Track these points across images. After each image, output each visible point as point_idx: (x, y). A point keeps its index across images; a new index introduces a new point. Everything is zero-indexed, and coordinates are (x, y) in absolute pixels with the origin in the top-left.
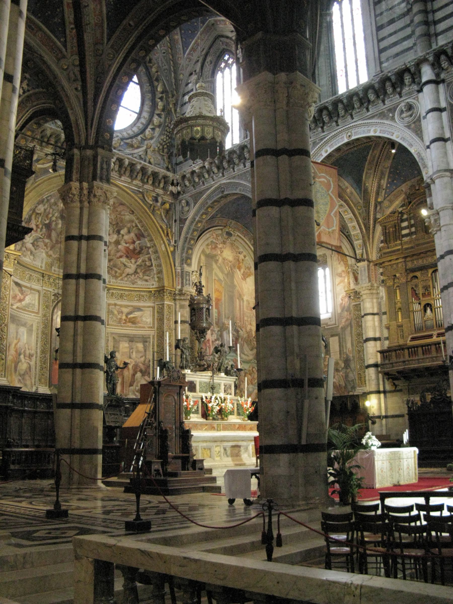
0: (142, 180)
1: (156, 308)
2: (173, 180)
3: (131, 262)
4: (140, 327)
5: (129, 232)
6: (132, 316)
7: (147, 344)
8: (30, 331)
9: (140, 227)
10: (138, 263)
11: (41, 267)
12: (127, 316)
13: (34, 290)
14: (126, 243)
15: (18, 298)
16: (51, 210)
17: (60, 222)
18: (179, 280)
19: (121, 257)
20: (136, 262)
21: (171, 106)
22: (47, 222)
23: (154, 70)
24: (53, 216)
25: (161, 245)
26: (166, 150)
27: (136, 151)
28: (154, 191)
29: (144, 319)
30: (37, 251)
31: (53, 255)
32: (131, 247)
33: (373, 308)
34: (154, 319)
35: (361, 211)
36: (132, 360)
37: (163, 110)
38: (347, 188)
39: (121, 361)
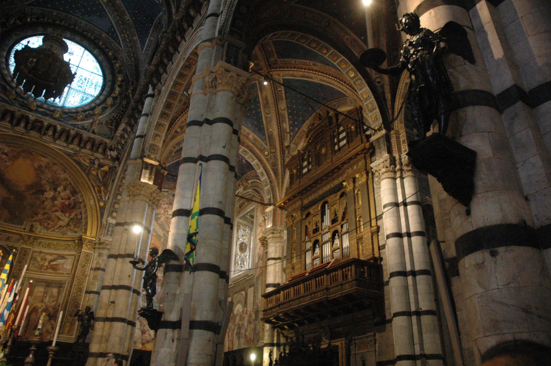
0: (79, 145)
2: (112, 146)
3: (65, 216)
4: (60, 273)
5: (65, 189)
6: (54, 263)
7: (62, 289)
9: (73, 185)
10: (71, 217)
12: (49, 263)
14: (62, 199)
18: (102, 231)
19: (56, 211)
20: (69, 216)
21: (129, 91)
23: (117, 65)
25: (89, 200)
26: (114, 124)
27: (79, 123)
28: (92, 155)
29: (65, 266)
32: (67, 203)
33: (276, 253)
35: (268, 157)
36: (43, 304)
37: (120, 94)
38: (249, 134)
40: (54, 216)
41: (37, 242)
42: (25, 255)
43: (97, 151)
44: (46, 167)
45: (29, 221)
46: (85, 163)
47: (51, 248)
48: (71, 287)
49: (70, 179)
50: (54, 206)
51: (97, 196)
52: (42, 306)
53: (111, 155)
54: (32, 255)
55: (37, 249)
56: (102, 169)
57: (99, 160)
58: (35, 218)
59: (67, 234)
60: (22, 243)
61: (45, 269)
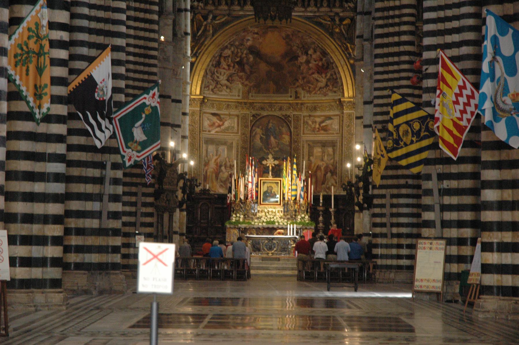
1: (341, 116)
3: (322, 77)
4: (331, 134)
5: (315, 52)
6: (324, 124)
7: (335, 148)
8: (230, 148)
11: (239, 96)
12: (320, 125)
13: (233, 115)
14: (315, 61)
15: (217, 124)
16: (239, 50)
17: (251, 56)
19: (313, 73)
20: (326, 76)
22: (238, 60)
24: (242, 53)
28: (331, 11)
29: (333, 126)
30: (232, 85)
31: (249, 84)
32: (320, 64)
34: (340, 126)
36: (324, 162)
39: (315, 164)
40: (312, 79)
41: (304, 107)
42: (298, 121)
43: (334, 6)
44: (292, 35)
45: (292, 88)
46: (326, 22)
47: (318, 110)
48: (342, 145)
49: (317, 43)
50: (310, 69)
51: (346, 55)
52: (323, 164)
53: (349, 6)
54: (304, 120)
55: (305, 113)
56: (344, 23)
57: (339, 16)
58: (297, 84)
59: (328, 94)
60: (293, 111)
61: (317, 131)
